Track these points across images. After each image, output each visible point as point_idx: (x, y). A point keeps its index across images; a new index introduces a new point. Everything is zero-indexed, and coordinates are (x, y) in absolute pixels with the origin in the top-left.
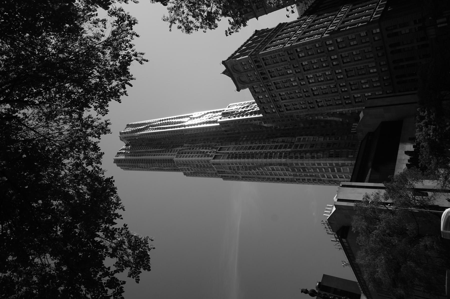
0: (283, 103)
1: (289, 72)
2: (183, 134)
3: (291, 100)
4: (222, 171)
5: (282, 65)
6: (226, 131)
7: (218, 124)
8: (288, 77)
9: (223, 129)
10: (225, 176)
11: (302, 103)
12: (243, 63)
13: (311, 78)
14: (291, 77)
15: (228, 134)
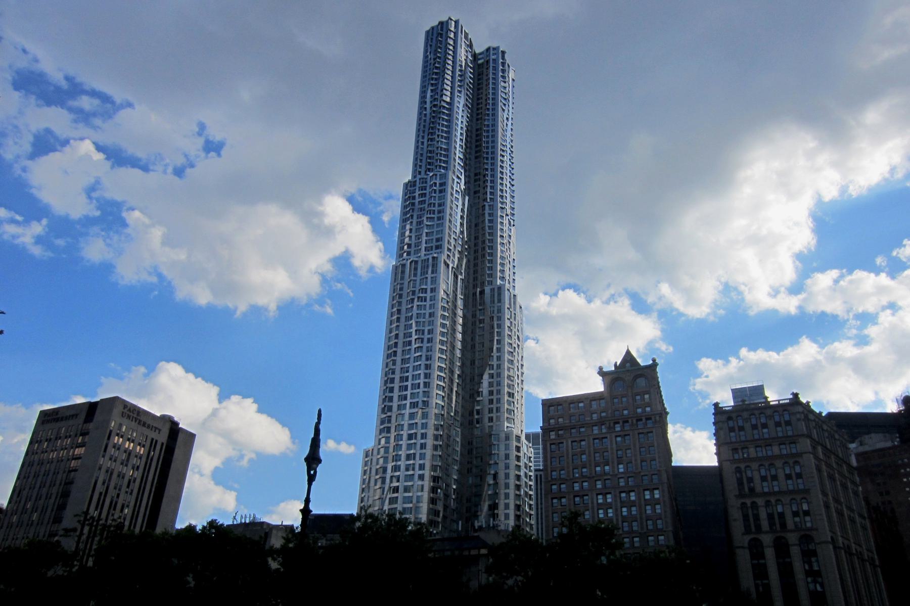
0: (567, 442)
1: (621, 466)
2: (485, 200)
3: (570, 456)
4: (416, 269)
5: (636, 460)
6: (482, 292)
7: (499, 282)
8: (613, 463)
9: (487, 289)
10: (403, 272)
11: (562, 472)
12: (647, 396)
13: (606, 499)
14: (613, 467)
15: (474, 294)
